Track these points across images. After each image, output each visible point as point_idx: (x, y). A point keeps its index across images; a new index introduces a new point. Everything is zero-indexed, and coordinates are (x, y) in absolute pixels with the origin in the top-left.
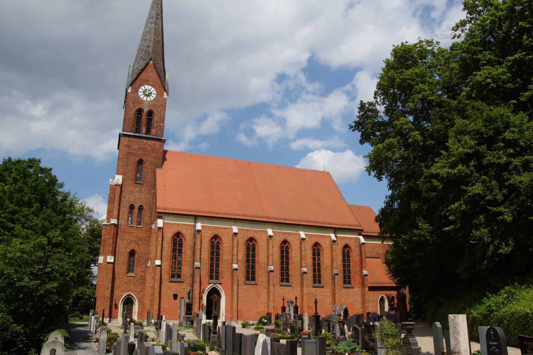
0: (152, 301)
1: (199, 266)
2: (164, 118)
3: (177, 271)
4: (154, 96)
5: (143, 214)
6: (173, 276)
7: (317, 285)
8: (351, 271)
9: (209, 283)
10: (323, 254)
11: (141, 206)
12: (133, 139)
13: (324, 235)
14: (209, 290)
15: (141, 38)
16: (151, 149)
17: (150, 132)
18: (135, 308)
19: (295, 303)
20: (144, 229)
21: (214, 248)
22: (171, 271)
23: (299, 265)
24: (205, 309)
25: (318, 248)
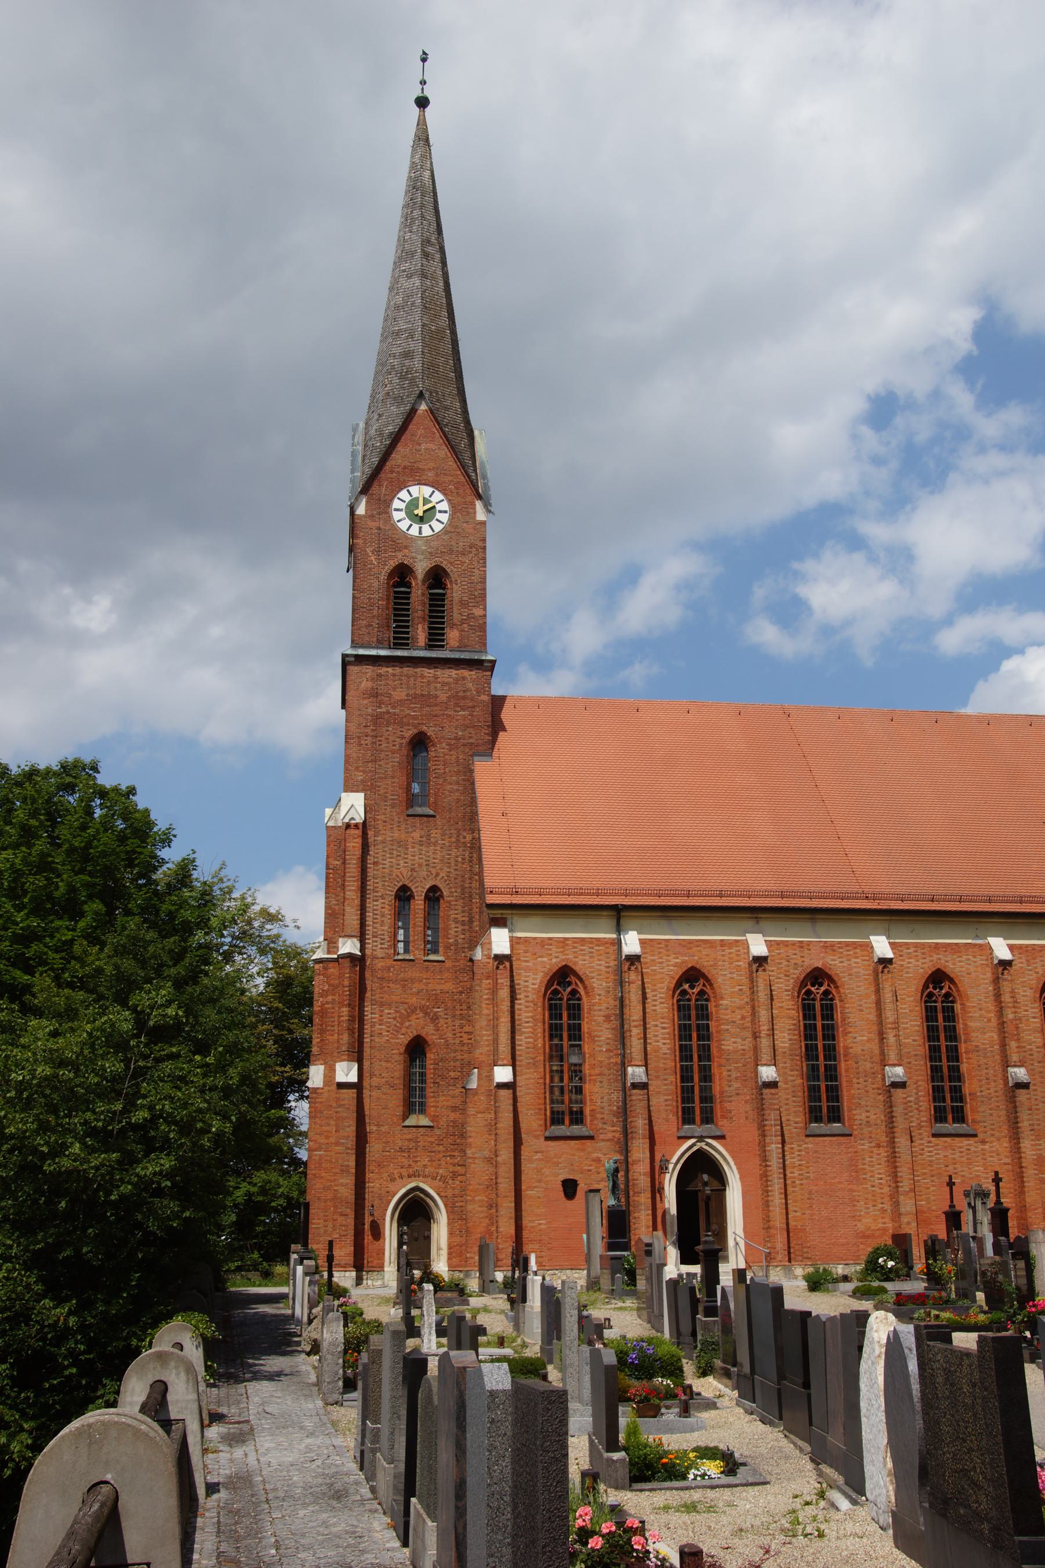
0: (493, 1205)
1: (644, 1079)
2: (484, 589)
4: (444, 518)
5: (441, 914)
6: (556, 1119)
9: (679, 1138)
11: (434, 889)
12: (390, 670)
14: (682, 1161)
16: (449, 698)
17: (443, 641)
18: (439, 1232)
19: (993, 1197)
20: (448, 964)
22: (548, 1101)
23: (998, 1057)
24: (673, 1227)
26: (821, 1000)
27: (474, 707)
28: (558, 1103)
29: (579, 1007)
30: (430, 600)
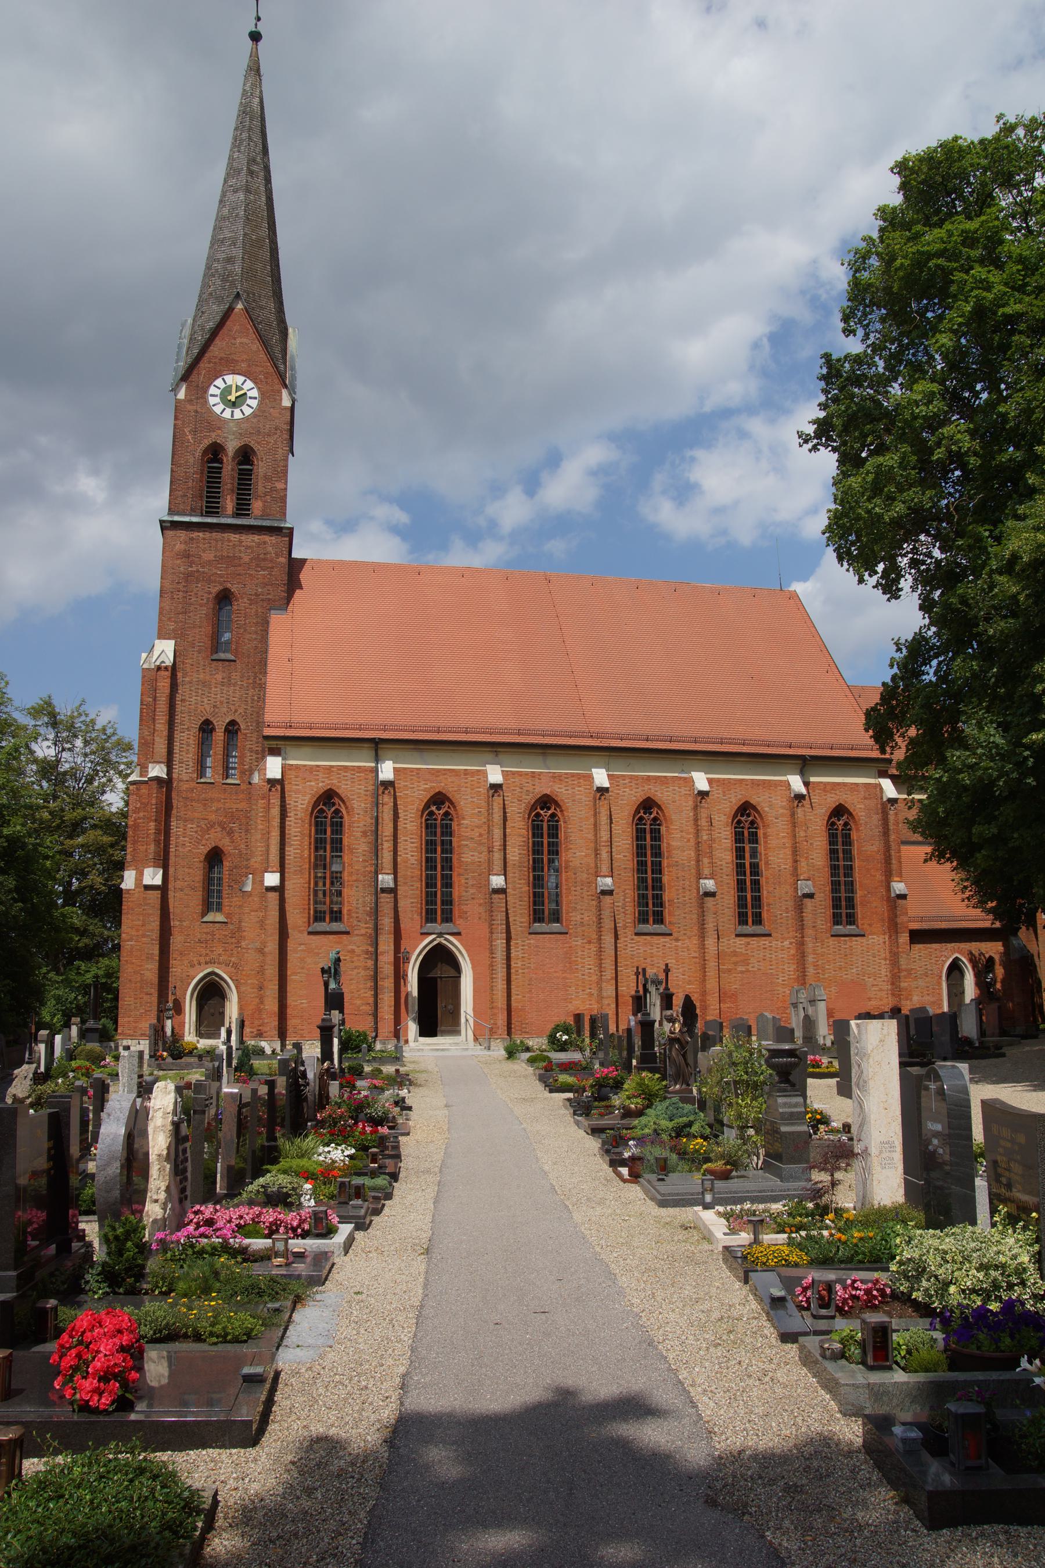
2: (286, 466)
3: (331, 902)
4: (254, 403)
7: (749, 929)
8: (857, 886)
9: (422, 934)
10: (765, 836)
11: (233, 723)
12: (201, 534)
13: (770, 781)
15: (210, 238)
16: (251, 559)
17: (249, 510)
21: (435, 832)
23: (693, 871)
24: (414, 1006)
25: (750, 819)
26: (549, 821)
27: (272, 568)
28: (321, 903)
29: (341, 824)
30: (239, 474)
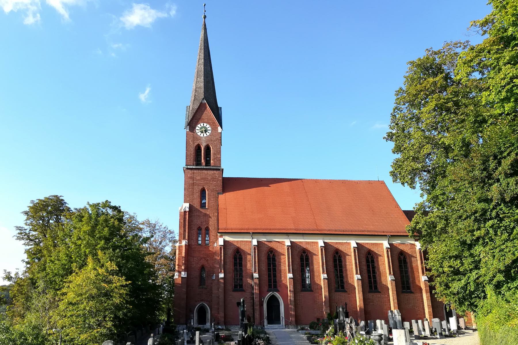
4: (210, 132)
6: (236, 286)
27: (218, 181)
29: (242, 258)
